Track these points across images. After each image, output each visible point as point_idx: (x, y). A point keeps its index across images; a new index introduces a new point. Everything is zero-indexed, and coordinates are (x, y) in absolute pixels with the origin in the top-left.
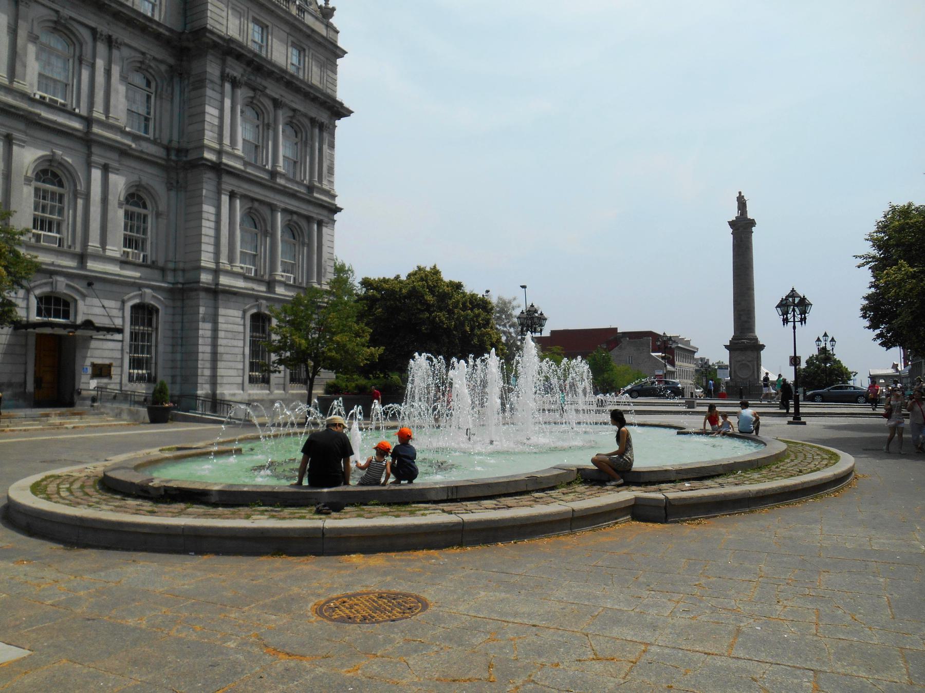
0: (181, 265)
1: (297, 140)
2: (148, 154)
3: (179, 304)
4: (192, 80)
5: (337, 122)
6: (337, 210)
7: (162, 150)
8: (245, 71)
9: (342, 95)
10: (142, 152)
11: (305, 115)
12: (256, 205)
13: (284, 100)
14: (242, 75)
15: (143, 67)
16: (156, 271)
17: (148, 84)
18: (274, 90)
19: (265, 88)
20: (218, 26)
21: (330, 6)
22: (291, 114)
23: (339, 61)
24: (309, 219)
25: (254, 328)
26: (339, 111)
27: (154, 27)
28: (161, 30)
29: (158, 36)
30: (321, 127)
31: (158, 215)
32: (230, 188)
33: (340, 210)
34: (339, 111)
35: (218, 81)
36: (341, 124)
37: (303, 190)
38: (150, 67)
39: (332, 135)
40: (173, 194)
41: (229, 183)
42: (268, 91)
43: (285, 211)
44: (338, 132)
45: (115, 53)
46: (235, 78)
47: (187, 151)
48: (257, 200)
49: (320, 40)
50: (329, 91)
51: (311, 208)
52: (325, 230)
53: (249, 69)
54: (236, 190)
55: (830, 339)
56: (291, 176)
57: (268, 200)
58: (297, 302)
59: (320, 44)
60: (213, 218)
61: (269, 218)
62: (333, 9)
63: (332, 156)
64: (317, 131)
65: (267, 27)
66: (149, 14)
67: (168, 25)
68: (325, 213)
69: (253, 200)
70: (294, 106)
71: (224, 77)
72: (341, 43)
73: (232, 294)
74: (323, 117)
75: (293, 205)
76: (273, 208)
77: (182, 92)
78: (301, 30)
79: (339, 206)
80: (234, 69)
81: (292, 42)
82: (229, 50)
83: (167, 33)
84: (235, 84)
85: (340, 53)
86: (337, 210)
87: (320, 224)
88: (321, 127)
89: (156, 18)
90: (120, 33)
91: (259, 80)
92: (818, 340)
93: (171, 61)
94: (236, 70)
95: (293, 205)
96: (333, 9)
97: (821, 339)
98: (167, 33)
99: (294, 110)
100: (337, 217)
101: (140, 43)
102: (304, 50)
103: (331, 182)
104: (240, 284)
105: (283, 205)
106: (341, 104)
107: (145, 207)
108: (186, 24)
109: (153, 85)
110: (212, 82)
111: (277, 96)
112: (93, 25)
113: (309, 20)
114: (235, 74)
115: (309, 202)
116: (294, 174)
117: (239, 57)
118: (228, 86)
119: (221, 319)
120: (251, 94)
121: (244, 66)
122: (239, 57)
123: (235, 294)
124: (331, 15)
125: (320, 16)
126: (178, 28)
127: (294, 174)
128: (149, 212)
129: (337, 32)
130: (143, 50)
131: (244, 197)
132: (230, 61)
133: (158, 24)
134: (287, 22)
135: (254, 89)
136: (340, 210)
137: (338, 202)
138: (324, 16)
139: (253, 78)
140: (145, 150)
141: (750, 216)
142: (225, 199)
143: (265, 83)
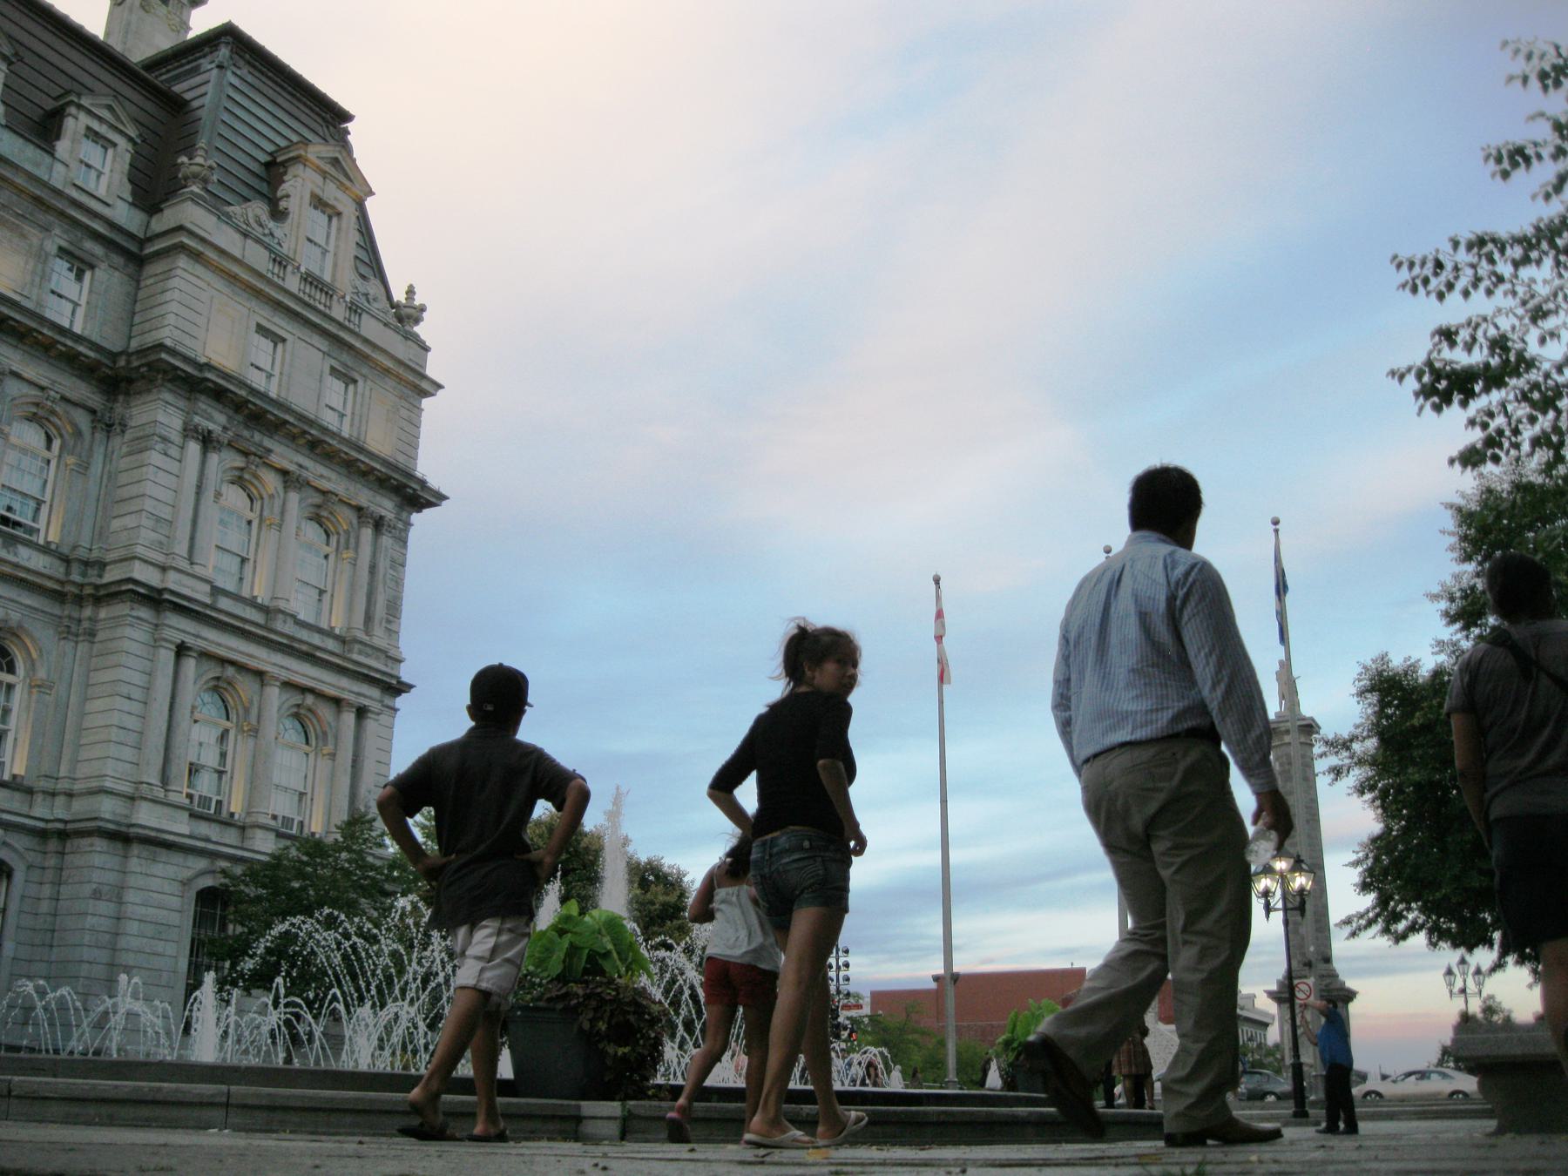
0: (63, 785)
1: (328, 550)
2: (28, 570)
3: (52, 861)
4: (128, 436)
5: (415, 518)
6: (397, 688)
7: (57, 563)
8: (230, 418)
9: (429, 467)
10: (16, 566)
12: (230, 671)
13: (305, 473)
14: (225, 428)
15: (41, 413)
16: (17, 795)
17: (49, 440)
18: (284, 455)
19: (269, 451)
20: (188, 341)
21: (417, 303)
22: (318, 499)
23: (426, 403)
24: (337, 702)
25: (200, 920)
26: (415, 496)
27: (69, 343)
28: (81, 349)
30: (378, 524)
32: (179, 637)
34: (415, 496)
35: (176, 437)
37: (331, 644)
38: (53, 412)
39: (403, 542)
40: (68, 646)
41: (179, 628)
42: (274, 459)
43: (288, 685)
44: (413, 535)
46: (210, 432)
47: (102, 565)
48: (232, 663)
49: (389, 364)
50: (401, 459)
51: (344, 682)
52: (370, 724)
53: (240, 418)
54: (189, 641)
55: (1472, 969)
56: (311, 620)
57: (253, 664)
58: (277, 860)
59: (387, 371)
60: (137, 694)
61: (256, 699)
62: (422, 309)
63: (399, 583)
64: (367, 533)
65: (284, 340)
66: (67, 325)
67: (95, 338)
68: (375, 692)
69: (224, 661)
70: (325, 485)
71: (189, 431)
72: (433, 369)
74: (385, 506)
75: (305, 673)
77: (107, 457)
78: (351, 347)
79: (405, 678)
80: (210, 418)
81: (333, 368)
82: (198, 383)
83: (92, 354)
84: (208, 442)
85: (425, 385)
86: (397, 688)
87: (361, 712)
88: (378, 524)
89: (77, 329)
91: (257, 437)
92: (1449, 972)
93: (95, 399)
94: (215, 419)
95: (305, 673)
96: (422, 309)
97: (1455, 970)
98: (92, 354)
99: (324, 493)
100: (401, 701)
101: (34, 370)
102: (355, 382)
103: (393, 633)
104: (179, 826)
105: (285, 675)
106: (423, 483)
107: (11, 669)
108: (130, 338)
109: (57, 444)
110: (165, 439)
111: (292, 468)
113: (370, 328)
114: (211, 426)
116: (319, 614)
117: (219, 395)
118: (194, 448)
119: (131, 896)
120: (239, 461)
121: (231, 413)
122: (219, 395)
124: (417, 321)
125: (394, 321)
126: (115, 344)
127: (319, 614)
128: (19, 678)
129: (426, 349)
130: (44, 383)
131: (205, 655)
132: (204, 404)
133: (79, 338)
134: (325, 333)
135: (246, 454)
137: (405, 673)
138: (400, 319)
139: (246, 433)
140: (26, 564)
141: (1307, 709)
142: (167, 656)
143: (267, 443)
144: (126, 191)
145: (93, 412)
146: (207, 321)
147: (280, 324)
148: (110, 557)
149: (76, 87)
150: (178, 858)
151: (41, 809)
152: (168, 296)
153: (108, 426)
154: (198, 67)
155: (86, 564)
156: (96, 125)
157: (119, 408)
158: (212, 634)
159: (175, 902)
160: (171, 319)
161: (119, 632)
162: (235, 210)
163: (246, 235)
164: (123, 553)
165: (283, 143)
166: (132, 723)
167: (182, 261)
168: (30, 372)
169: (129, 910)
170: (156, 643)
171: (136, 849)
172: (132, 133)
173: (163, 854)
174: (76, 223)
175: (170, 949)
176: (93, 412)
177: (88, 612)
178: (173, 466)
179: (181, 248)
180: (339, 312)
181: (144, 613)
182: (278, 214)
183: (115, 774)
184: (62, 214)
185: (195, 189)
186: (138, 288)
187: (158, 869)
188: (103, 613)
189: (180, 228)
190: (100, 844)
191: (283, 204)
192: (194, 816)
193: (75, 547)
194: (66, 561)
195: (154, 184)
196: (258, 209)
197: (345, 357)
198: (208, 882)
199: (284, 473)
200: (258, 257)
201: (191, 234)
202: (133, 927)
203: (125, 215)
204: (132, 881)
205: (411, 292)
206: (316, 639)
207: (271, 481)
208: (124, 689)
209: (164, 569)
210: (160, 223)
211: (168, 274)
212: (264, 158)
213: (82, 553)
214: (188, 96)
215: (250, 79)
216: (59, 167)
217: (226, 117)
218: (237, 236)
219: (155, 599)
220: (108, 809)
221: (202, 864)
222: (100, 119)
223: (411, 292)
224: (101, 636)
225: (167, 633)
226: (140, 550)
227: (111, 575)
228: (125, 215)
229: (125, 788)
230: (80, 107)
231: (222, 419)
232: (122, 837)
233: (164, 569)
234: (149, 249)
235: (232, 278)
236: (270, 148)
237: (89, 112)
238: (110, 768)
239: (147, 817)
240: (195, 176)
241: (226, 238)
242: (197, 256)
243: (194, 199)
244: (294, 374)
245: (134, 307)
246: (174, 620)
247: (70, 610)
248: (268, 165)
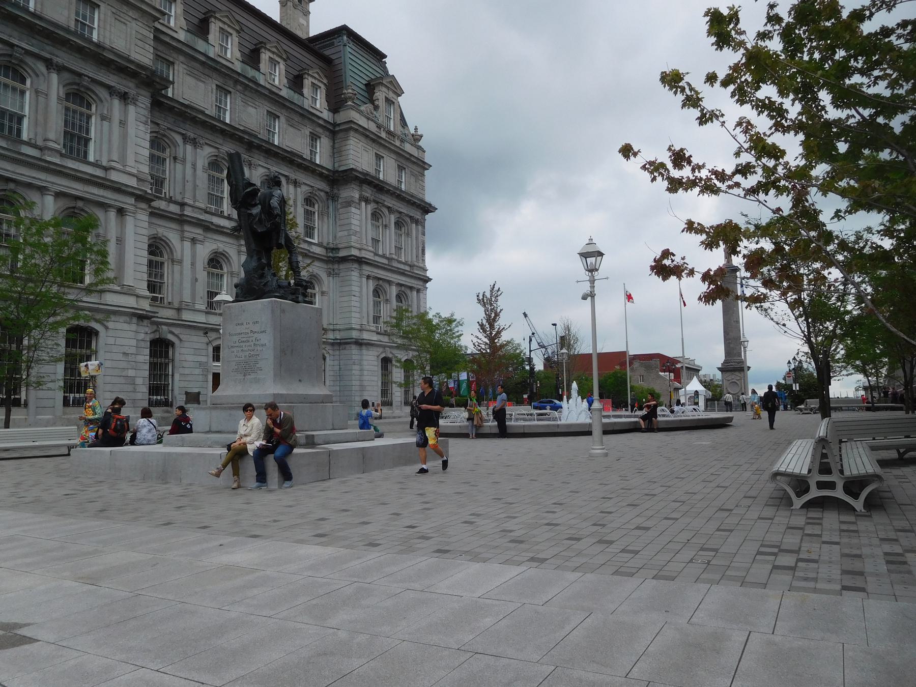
5: (427, 217)
6: (428, 280)
9: (429, 197)
11: (407, 215)
18: (389, 202)
21: (419, 133)
22: (398, 215)
24: (411, 288)
29: (321, 175)
30: (417, 222)
31: (323, 293)
32: (367, 273)
33: (430, 280)
36: (428, 217)
37: (407, 268)
39: (424, 227)
40: (331, 278)
41: (367, 270)
45: (298, 189)
47: (338, 249)
48: (381, 279)
50: (421, 195)
51: (413, 281)
52: (421, 295)
60: (357, 294)
64: (414, 225)
68: (421, 283)
69: (379, 279)
73: (369, 344)
74: (417, 215)
76: (390, 282)
78: (403, 156)
86: (428, 280)
87: (418, 291)
90: (301, 177)
91: (380, 196)
93: (327, 189)
94: (368, 192)
99: (400, 213)
100: (428, 285)
103: (424, 260)
104: (375, 337)
105: (397, 281)
112: (286, 174)
115: (411, 277)
118: (363, 204)
119: (365, 363)
123: (372, 345)
132: (365, 187)
135: (377, 203)
136: (430, 280)
137: (428, 274)
142: (364, 280)
143: (383, 198)
144: (325, 105)
145: (327, 193)
146: (359, 156)
147: (382, 152)
148: (340, 246)
149: (308, 67)
150: (375, 349)
151: (331, 336)
152: (348, 147)
153: (332, 197)
154: (333, 44)
155: (333, 249)
156: (316, 82)
157: (336, 191)
158: (376, 271)
159: (376, 363)
160: (351, 157)
161: (349, 273)
162: (362, 108)
163: (368, 119)
164: (346, 245)
165: (373, 77)
166: (357, 304)
167: (352, 133)
168: (308, 182)
169: (366, 367)
170: (361, 276)
171: (364, 347)
172: (325, 81)
173: (371, 348)
174: (314, 121)
175: (375, 378)
176: (327, 193)
177: (336, 266)
178: (358, 212)
179: (351, 128)
180: (398, 143)
181: (356, 265)
182: (376, 108)
183: (355, 322)
184: (309, 119)
185: (350, 103)
186: (334, 143)
187: (370, 353)
188: (341, 266)
189: (351, 121)
190: (353, 347)
191: (376, 103)
192: (378, 333)
193: (328, 244)
194: (326, 249)
195: (336, 103)
196: (370, 106)
197: (400, 160)
198: (383, 355)
199: (389, 208)
200: (372, 127)
201: (355, 123)
202: (365, 373)
203: (326, 115)
204: (365, 358)
205: (416, 129)
206: (402, 266)
207: (386, 211)
208: (354, 293)
209: (360, 249)
210: (341, 117)
211: (347, 139)
212: (364, 82)
213: (331, 246)
214: (333, 57)
215: (354, 47)
216: (305, 100)
217: (350, 67)
218: (365, 120)
219: (360, 261)
220: (355, 334)
221: (381, 350)
222: (315, 78)
223: (416, 129)
224: (341, 274)
225: (364, 272)
226: (353, 244)
227: (342, 254)
228: (326, 115)
229: (358, 327)
230: (309, 75)
231: (369, 191)
232: (359, 343)
233: (360, 249)
234: (337, 129)
235: (367, 137)
236: (368, 79)
237: (312, 76)
238: (353, 321)
239: (366, 336)
240: (350, 98)
241: (363, 122)
242: (356, 131)
243: (352, 108)
244: (388, 172)
245: (336, 152)
246: (365, 267)
247: (330, 266)
248: (366, 85)
